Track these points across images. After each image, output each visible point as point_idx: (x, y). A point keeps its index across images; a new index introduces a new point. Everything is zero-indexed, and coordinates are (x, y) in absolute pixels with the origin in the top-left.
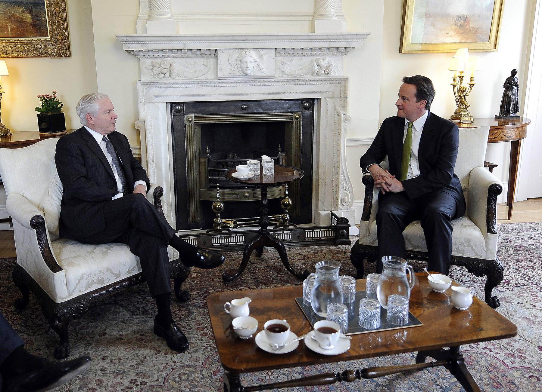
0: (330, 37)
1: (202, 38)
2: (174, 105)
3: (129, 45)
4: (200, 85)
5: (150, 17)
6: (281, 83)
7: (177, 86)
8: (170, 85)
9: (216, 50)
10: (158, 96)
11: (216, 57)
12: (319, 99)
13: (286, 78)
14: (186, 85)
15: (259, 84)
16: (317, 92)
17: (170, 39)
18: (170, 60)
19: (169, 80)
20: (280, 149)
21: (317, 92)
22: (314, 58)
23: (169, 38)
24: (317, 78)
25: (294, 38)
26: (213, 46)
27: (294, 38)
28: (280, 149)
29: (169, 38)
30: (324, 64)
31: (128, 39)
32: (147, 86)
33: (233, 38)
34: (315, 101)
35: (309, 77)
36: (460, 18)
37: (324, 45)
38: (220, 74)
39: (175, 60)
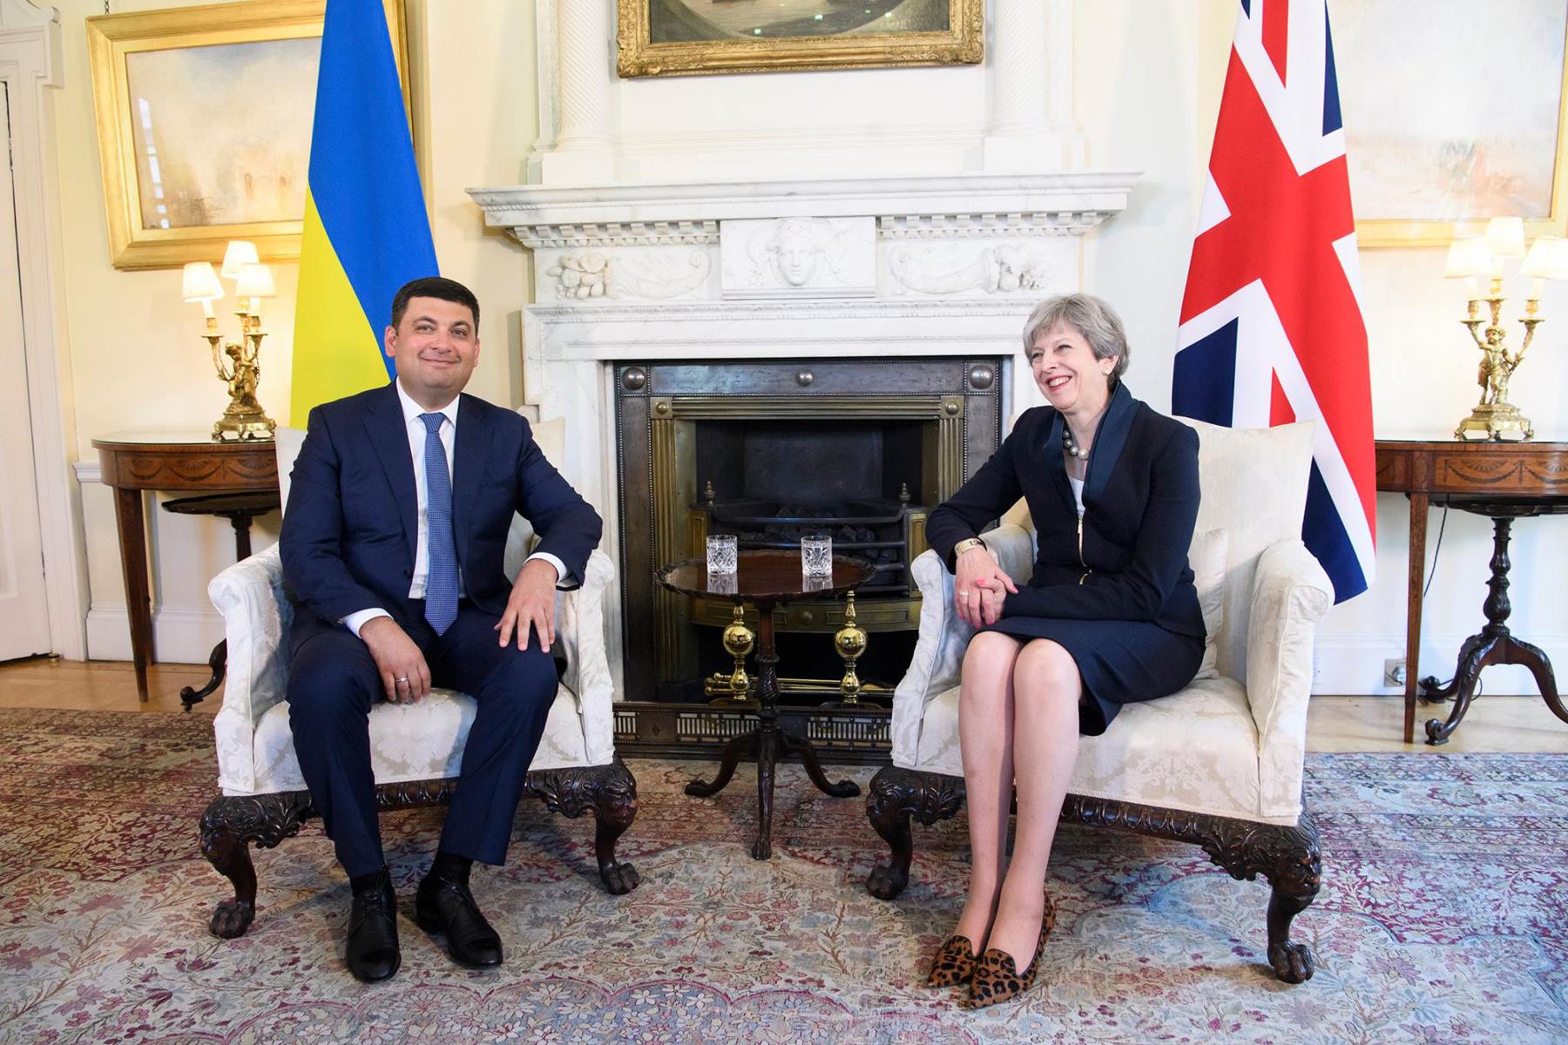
0: (1023, 182)
1: (677, 192)
2: (623, 369)
3: (499, 214)
4: (679, 316)
5: (553, 146)
6: (898, 312)
7: (623, 316)
8: (603, 316)
9: (718, 222)
10: (576, 344)
11: (717, 242)
12: (1011, 357)
13: (912, 296)
14: (643, 316)
15: (836, 313)
16: (1002, 338)
17: (597, 196)
18: (606, 252)
19: (605, 302)
20: (905, 496)
21: (1002, 338)
22: (991, 244)
23: (594, 194)
24: (999, 296)
25: (921, 185)
26: (708, 212)
27: (921, 185)
28: (905, 496)
29: (594, 194)
30: (1017, 263)
31: (498, 199)
32: (548, 318)
33: (758, 189)
34: (1007, 365)
35: (979, 294)
36: (1451, 148)
37: (1013, 203)
38: (728, 284)
39: (619, 252)
